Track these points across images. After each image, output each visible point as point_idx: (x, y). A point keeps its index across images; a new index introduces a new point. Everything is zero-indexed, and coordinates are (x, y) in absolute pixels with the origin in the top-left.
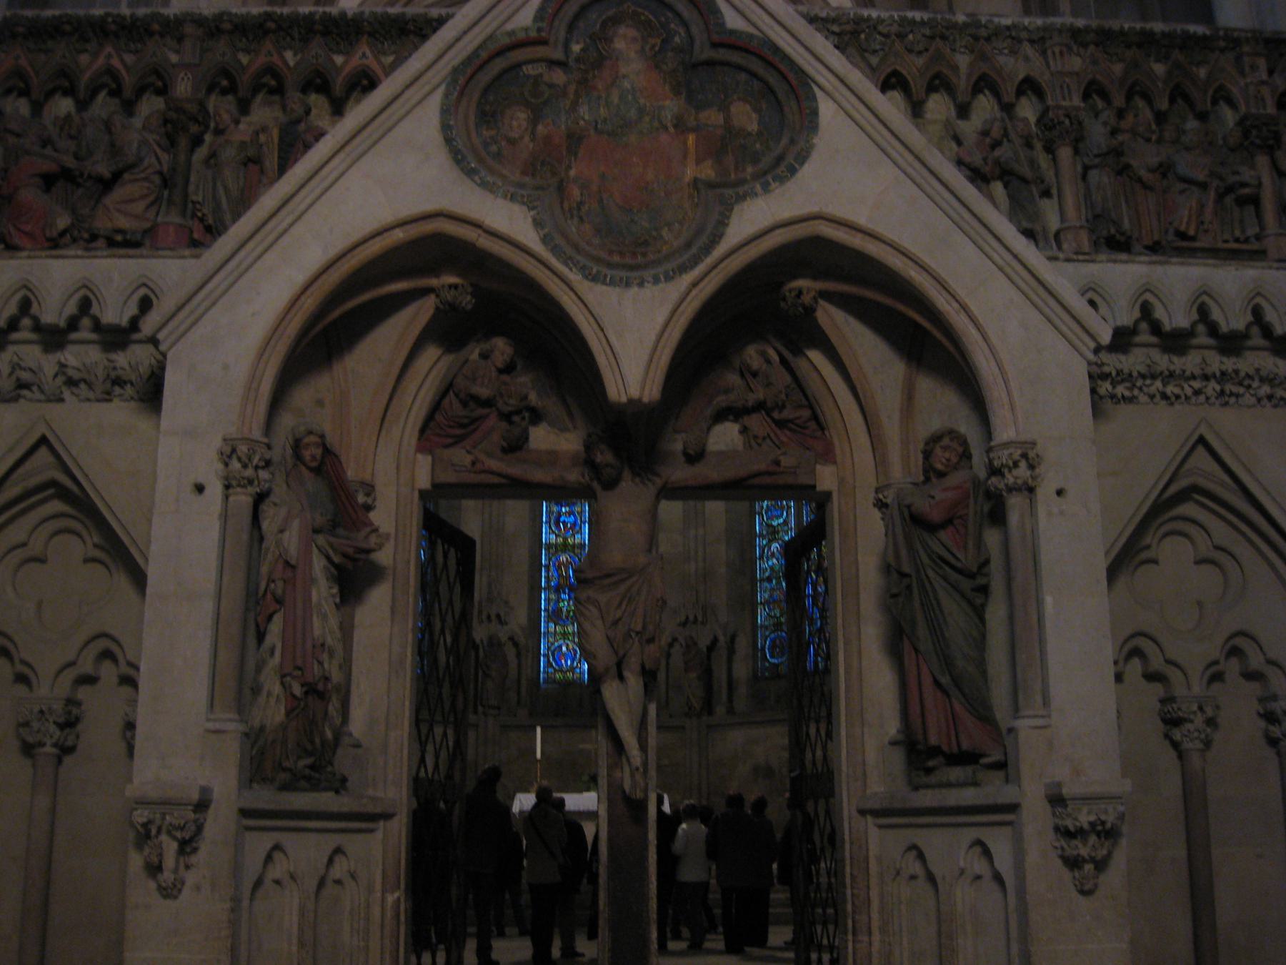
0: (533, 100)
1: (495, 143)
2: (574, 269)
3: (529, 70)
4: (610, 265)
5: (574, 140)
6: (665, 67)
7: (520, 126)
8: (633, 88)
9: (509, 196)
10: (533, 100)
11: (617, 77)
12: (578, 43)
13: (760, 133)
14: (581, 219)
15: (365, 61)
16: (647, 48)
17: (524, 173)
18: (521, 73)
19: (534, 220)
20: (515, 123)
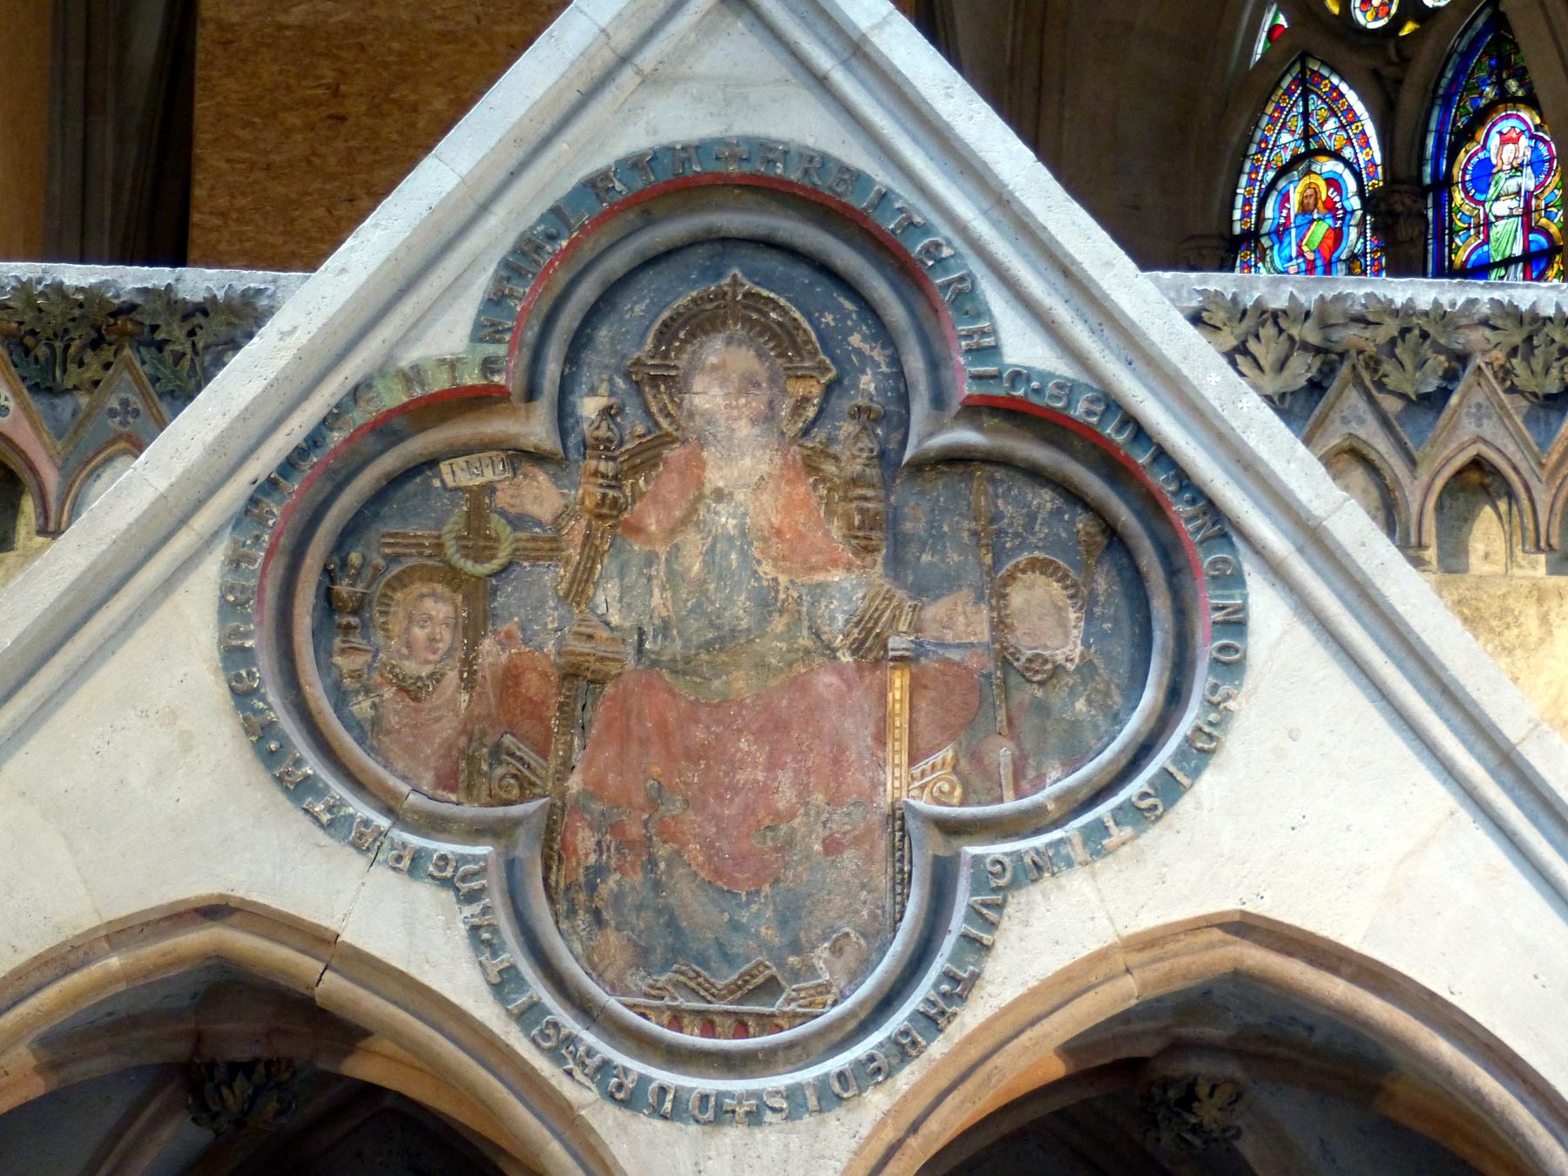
0: (469, 566)
1: (367, 691)
2: (578, 1075)
3: (455, 474)
6: (830, 468)
7: (432, 640)
8: (743, 534)
9: (406, 863)
10: (469, 566)
12: (593, 392)
14: (596, 914)
17: (447, 781)
18: (437, 483)
19: (474, 930)
20: (419, 633)
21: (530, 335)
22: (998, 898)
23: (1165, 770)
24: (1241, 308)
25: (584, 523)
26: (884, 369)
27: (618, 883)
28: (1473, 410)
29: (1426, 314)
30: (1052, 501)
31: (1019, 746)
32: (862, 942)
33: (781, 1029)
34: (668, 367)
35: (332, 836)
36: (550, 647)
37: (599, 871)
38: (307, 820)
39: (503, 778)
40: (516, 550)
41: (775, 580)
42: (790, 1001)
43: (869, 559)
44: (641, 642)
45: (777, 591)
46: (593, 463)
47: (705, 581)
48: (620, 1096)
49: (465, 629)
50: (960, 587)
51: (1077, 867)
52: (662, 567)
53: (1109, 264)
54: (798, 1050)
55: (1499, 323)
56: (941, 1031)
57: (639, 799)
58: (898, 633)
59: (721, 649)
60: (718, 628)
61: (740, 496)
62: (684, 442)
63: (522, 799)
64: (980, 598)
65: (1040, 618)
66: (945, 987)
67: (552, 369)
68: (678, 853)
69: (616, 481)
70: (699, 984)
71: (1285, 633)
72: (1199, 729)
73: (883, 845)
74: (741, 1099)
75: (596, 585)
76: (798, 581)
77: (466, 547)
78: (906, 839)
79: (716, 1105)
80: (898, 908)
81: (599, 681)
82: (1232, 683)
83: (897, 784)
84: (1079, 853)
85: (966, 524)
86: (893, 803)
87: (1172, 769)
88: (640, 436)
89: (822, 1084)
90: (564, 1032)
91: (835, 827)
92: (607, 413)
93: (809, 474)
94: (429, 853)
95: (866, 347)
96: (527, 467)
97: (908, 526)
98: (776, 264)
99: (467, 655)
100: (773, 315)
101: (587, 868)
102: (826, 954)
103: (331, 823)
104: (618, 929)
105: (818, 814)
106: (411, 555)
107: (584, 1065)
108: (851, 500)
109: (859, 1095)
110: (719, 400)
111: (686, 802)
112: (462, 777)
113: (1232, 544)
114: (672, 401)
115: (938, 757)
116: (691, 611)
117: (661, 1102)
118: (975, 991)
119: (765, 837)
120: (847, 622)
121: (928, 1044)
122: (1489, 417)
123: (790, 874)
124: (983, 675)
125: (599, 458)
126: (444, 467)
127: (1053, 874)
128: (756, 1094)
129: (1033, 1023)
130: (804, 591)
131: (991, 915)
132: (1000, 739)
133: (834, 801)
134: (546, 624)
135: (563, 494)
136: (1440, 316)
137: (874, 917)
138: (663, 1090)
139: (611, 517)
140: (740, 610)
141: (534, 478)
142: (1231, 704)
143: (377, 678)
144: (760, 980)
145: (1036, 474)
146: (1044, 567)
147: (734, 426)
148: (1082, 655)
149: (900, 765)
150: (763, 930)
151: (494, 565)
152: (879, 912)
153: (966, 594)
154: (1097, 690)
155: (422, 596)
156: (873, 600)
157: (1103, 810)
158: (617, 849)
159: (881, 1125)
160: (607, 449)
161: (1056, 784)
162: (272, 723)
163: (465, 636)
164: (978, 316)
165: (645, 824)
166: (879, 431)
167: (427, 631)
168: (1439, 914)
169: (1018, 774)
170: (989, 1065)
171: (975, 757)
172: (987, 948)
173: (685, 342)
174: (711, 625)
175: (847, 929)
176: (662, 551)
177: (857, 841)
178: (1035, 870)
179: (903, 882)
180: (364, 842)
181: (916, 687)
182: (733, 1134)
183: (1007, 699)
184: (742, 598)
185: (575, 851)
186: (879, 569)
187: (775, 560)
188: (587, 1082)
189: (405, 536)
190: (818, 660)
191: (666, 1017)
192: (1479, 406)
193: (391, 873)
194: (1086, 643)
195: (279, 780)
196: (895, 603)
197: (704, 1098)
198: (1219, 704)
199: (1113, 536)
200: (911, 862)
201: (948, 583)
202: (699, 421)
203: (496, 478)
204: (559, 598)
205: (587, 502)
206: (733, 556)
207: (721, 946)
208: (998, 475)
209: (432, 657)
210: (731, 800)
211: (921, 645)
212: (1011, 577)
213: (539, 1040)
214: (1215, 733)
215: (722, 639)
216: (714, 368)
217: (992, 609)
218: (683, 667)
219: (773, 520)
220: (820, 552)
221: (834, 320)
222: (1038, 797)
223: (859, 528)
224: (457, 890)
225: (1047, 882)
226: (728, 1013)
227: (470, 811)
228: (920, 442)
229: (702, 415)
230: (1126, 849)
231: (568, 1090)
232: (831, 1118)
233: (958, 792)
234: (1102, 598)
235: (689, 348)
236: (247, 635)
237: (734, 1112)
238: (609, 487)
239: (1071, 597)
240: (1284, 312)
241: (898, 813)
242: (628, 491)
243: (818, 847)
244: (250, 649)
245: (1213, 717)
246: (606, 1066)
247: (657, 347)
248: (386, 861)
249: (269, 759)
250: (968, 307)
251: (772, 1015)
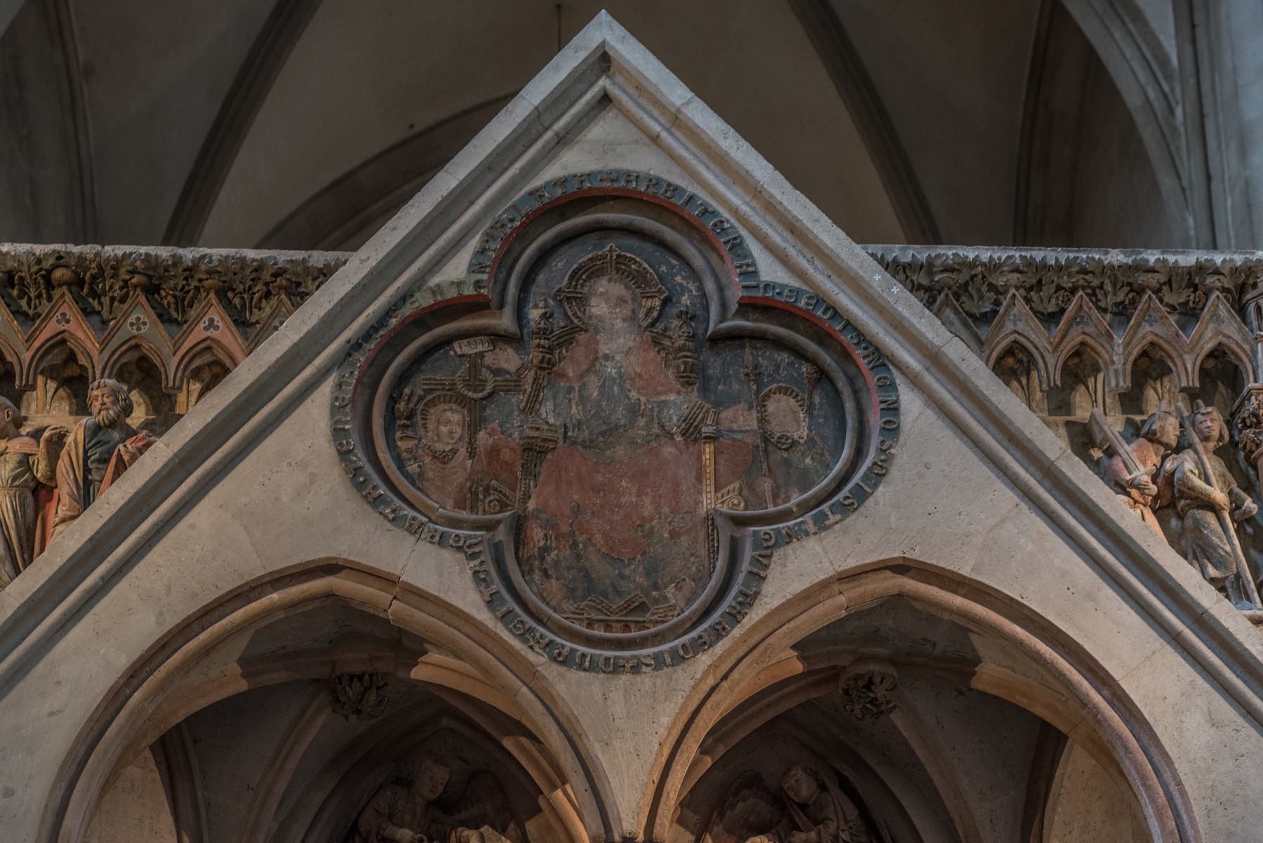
0: (470, 394)
1: (415, 459)
3: (463, 348)
4: (590, 641)
5: (535, 451)
6: (667, 343)
7: (451, 432)
8: (621, 376)
9: (437, 539)
10: (470, 394)
11: (596, 359)
12: (536, 306)
13: (810, 441)
14: (546, 574)
15: (211, 333)
16: (641, 315)
17: (460, 505)
18: (452, 353)
19: (476, 573)
20: (444, 429)
21: (501, 277)
22: (768, 552)
23: (858, 484)
24: (886, 262)
25: (533, 372)
26: (694, 293)
27: (557, 555)
28: (1012, 317)
29: (984, 265)
30: (788, 358)
31: (775, 482)
32: (693, 584)
33: (648, 628)
34: (577, 293)
35: (395, 526)
36: (516, 435)
37: (546, 549)
38: (381, 518)
39: (490, 502)
40: (496, 386)
41: (639, 399)
42: (653, 614)
43: (690, 389)
44: (566, 432)
45: (640, 406)
46: (537, 341)
47: (600, 401)
48: (561, 659)
49: (469, 426)
50: (740, 402)
51: (811, 535)
52: (577, 394)
53: (817, 221)
54: (659, 637)
55: (1025, 269)
56: (739, 622)
57: (567, 512)
58: (707, 425)
59: (610, 435)
60: (608, 424)
61: (618, 358)
62: (586, 331)
63: (501, 511)
64: (750, 408)
65: (784, 417)
66: (740, 599)
67: (512, 289)
68: (590, 539)
69: (550, 350)
70: (603, 607)
71: (921, 414)
72: (875, 463)
73: (702, 533)
74: (627, 660)
75: (541, 403)
76: (651, 400)
77: (467, 385)
78: (715, 531)
79: (614, 664)
80: (711, 565)
81: (543, 452)
82: (893, 439)
83: (709, 502)
84: (811, 528)
85: (742, 370)
86: (707, 512)
87: (861, 484)
88: (562, 328)
89: (673, 652)
90: (527, 626)
91: (676, 525)
92: (544, 316)
93: (655, 346)
94: (450, 534)
95: (684, 283)
96: (501, 344)
97: (710, 372)
98: (634, 242)
99: (470, 439)
100: (633, 266)
101: (539, 548)
102: (673, 590)
103: (394, 519)
104: (557, 579)
105: (666, 518)
106: (439, 390)
107: (538, 642)
108: (679, 358)
109: (695, 656)
110: (605, 310)
111: (593, 513)
112: (468, 502)
113: (889, 370)
114: (580, 310)
115: (731, 487)
116: (592, 416)
117: (582, 662)
118: (757, 601)
119: (637, 530)
120: (679, 420)
121: (732, 629)
122: (1021, 321)
123: (652, 549)
124: (754, 446)
125: (541, 339)
126: (456, 345)
127: (798, 540)
128: (635, 657)
129: (789, 621)
130: (655, 405)
131: (765, 561)
132: (765, 479)
133: (674, 511)
134: (513, 424)
135: (521, 358)
136: (993, 267)
137: (698, 570)
138: (584, 656)
139: (548, 369)
140: (620, 415)
141: (505, 350)
142: (893, 451)
143: (420, 452)
144: (636, 604)
145: (779, 343)
146: (786, 391)
147: (614, 322)
148: (808, 435)
149: (710, 492)
150: (638, 579)
151: (485, 393)
152: (701, 568)
153: (743, 406)
154: (817, 453)
155: (445, 411)
156: (693, 408)
157: (825, 507)
158: (556, 538)
159: (706, 674)
160: (544, 333)
161: (796, 498)
162: (360, 468)
163: (469, 430)
164: (746, 257)
165: (571, 525)
166: (693, 324)
167: (448, 428)
168: (1013, 557)
169: (775, 496)
170: (766, 643)
171: (751, 487)
172: (764, 578)
173: (585, 281)
174: (604, 422)
175: (684, 577)
176: (576, 386)
177: (688, 532)
178: (789, 537)
179: (714, 552)
180: (414, 529)
181: (716, 453)
182: (625, 678)
183: (767, 458)
184: (621, 409)
185: (532, 539)
186: (695, 393)
187: (638, 389)
188: (539, 651)
189: (435, 380)
190: (664, 440)
191: (585, 623)
192: (1015, 315)
193: (429, 545)
194: (809, 429)
195: (366, 497)
196: (704, 410)
197: (607, 659)
198: (886, 450)
199: (822, 376)
200: (718, 542)
201: (734, 400)
202: (594, 321)
203: (485, 350)
204: (520, 410)
205: (534, 361)
206: (615, 388)
207: (614, 587)
208: (758, 346)
209: (451, 441)
210: (618, 512)
211: (720, 431)
212: (767, 396)
213: (513, 629)
214: (885, 465)
215: (611, 429)
216: (602, 294)
217: (758, 412)
218: (589, 445)
219: (637, 369)
220: (663, 385)
221: (667, 269)
222: (788, 505)
223: (684, 372)
224: (466, 553)
225: (795, 543)
226: (620, 621)
227: (473, 517)
228: (716, 325)
229: (596, 317)
230: (838, 526)
231: (531, 657)
232: (679, 669)
233: (742, 505)
234: (818, 406)
235: (588, 283)
236: (346, 423)
237: (624, 666)
238: (546, 352)
239: (800, 406)
240: (910, 264)
241: (710, 517)
242: (557, 356)
243: (666, 535)
244: (349, 429)
245: (882, 457)
246: (551, 643)
247: (570, 283)
248: (425, 539)
249: (359, 486)
250: (740, 252)
251: (644, 622)
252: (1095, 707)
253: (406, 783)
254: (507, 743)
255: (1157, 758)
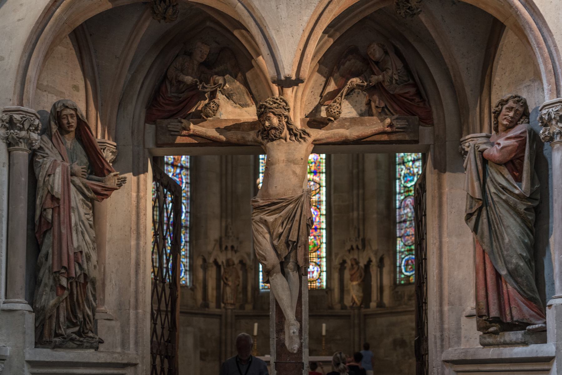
252: (517, 8)
253: (190, 54)
254: (236, 33)
255: (546, 34)
